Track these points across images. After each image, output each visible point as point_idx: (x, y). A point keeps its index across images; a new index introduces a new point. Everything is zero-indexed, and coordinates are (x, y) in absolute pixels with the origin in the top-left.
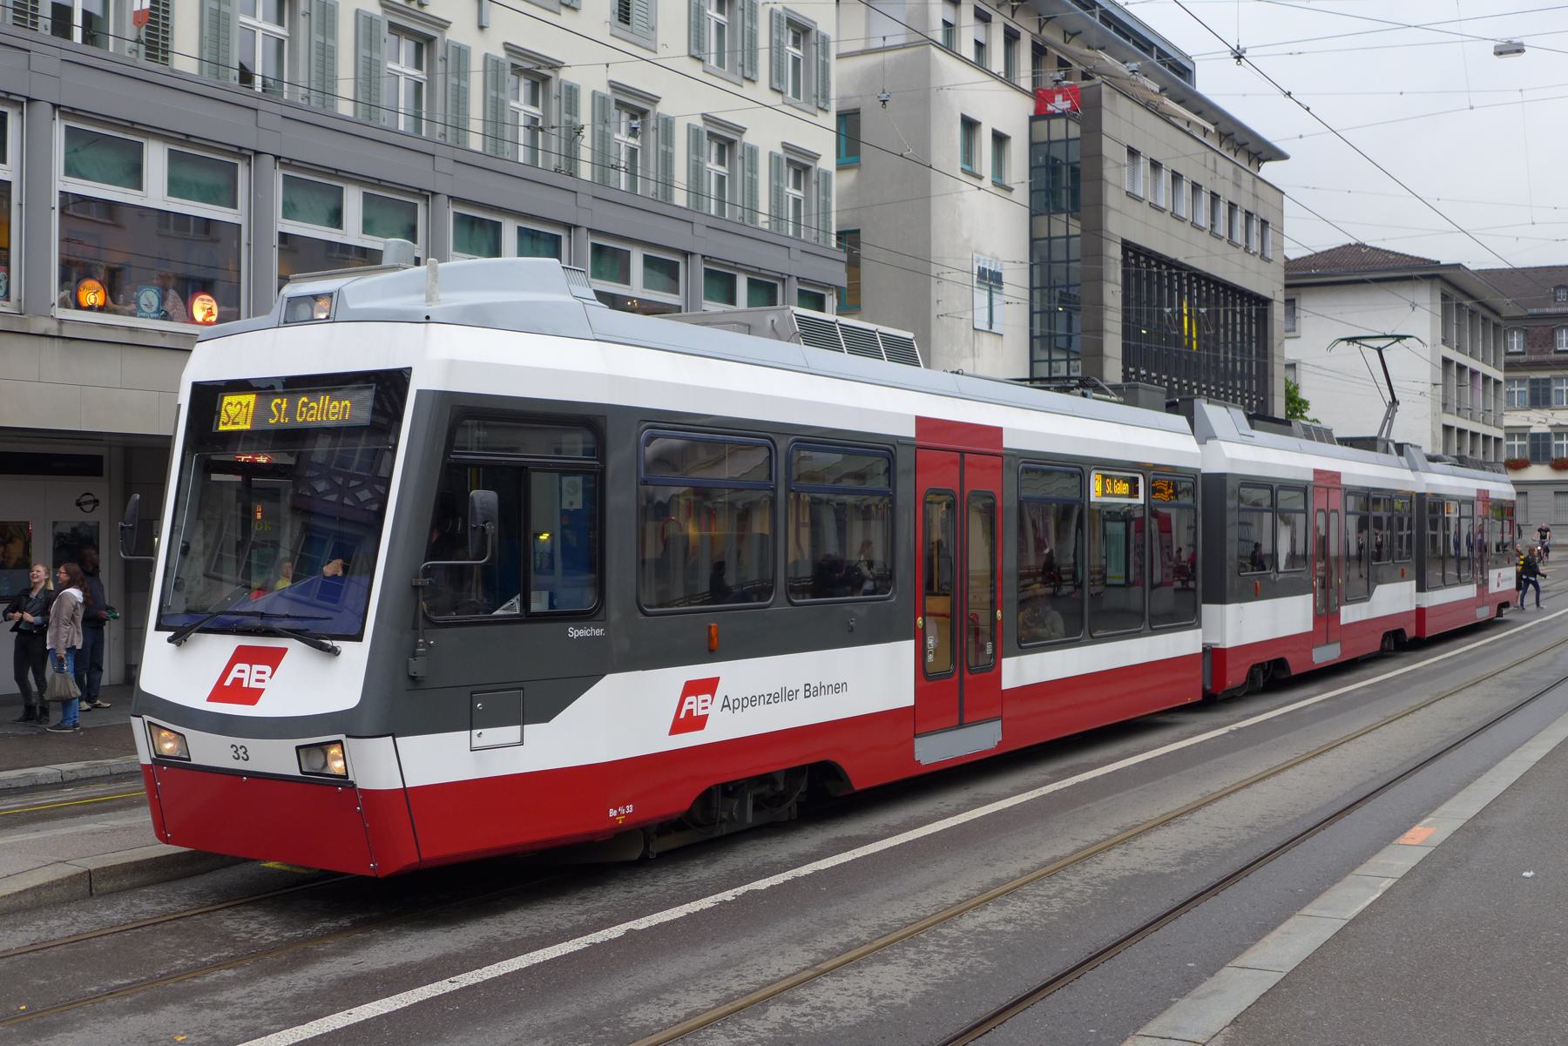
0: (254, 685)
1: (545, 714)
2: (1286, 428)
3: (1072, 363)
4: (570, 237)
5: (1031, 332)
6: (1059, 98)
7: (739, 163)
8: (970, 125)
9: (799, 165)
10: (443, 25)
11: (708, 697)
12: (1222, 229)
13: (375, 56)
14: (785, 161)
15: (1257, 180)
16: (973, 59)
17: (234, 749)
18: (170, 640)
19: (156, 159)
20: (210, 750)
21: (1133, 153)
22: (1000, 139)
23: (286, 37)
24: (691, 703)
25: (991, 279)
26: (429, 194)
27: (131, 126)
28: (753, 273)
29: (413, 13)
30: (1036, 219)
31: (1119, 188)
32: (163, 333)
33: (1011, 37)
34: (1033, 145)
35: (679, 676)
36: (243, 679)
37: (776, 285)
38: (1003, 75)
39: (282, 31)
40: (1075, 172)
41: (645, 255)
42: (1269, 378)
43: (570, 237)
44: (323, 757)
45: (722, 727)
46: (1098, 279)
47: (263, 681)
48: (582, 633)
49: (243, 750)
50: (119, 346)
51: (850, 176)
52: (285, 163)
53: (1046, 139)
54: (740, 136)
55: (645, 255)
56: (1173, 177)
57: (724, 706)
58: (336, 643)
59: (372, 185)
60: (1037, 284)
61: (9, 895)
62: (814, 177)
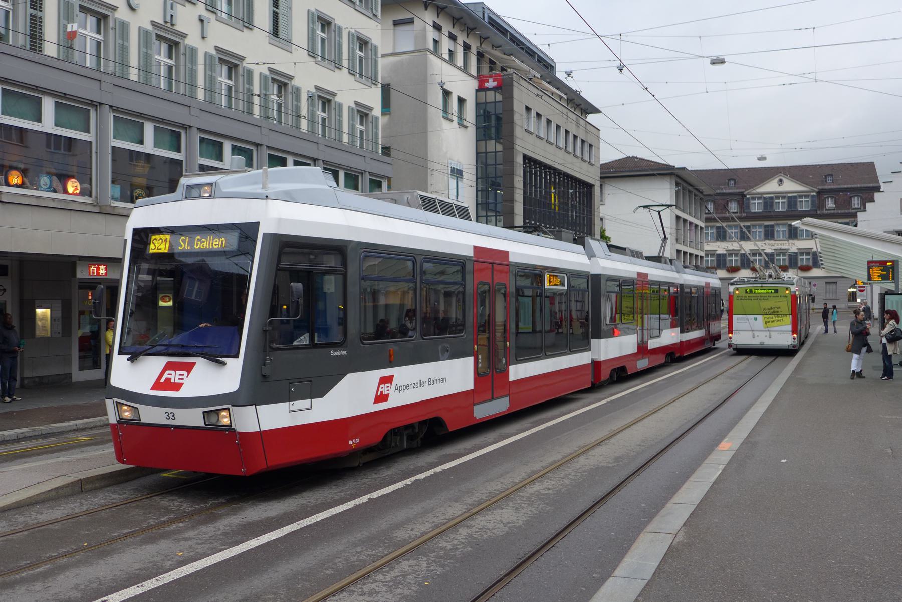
0: (177, 381)
1: (321, 394)
2: (624, 251)
3: (498, 217)
4: (257, 150)
5: (477, 201)
6: (491, 80)
7: (333, 112)
8: (447, 94)
9: (363, 113)
10: (184, 36)
11: (389, 385)
12: (570, 149)
13: (149, 52)
14: (356, 110)
15: (588, 124)
16: (448, 59)
18: (128, 360)
19: (48, 106)
20: (151, 415)
21: (528, 109)
22: (461, 101)
23: (102, 40)
24: (382, 388)
25: (457, 173)
26: (188, 127)
27: (36, 89)
28: (347, 170)
29: (167, 28)
30: (479, 142)
31: (522, 127)
32: (53, 199)
33: (467, 47)
34: (477, 104)
35: (376, 375)
37: (358, 176)
38: (462, 68)
39: (100, 37)
40: (498, 119)
41: (294, 160)
42: (593, 225)
43: (257, 150)
44: (217, 416)
45: (396, 400)
46: (511, 174)
47: (183, 379)
48: (337, 353)
49: (173, 414)
50: (30, 207)
51: (386, 118)
52: (115, 110)
53: (484, 101)
54: (334, 98)
55: (294, 160)
56: (547, 122)
57: (396, 390)
58: (224, 359)
59: (159, 122)
60: (479, 176)
61: (44, 492)
62: (370, 119)
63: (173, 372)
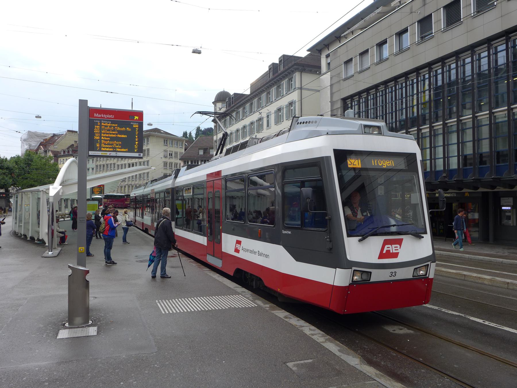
0: (394, 251)
17: (392, 273)
20: (378, 276)
36: (390, 250)
47: (398, 250)
58: (422, 235)
63: (390, 246)
